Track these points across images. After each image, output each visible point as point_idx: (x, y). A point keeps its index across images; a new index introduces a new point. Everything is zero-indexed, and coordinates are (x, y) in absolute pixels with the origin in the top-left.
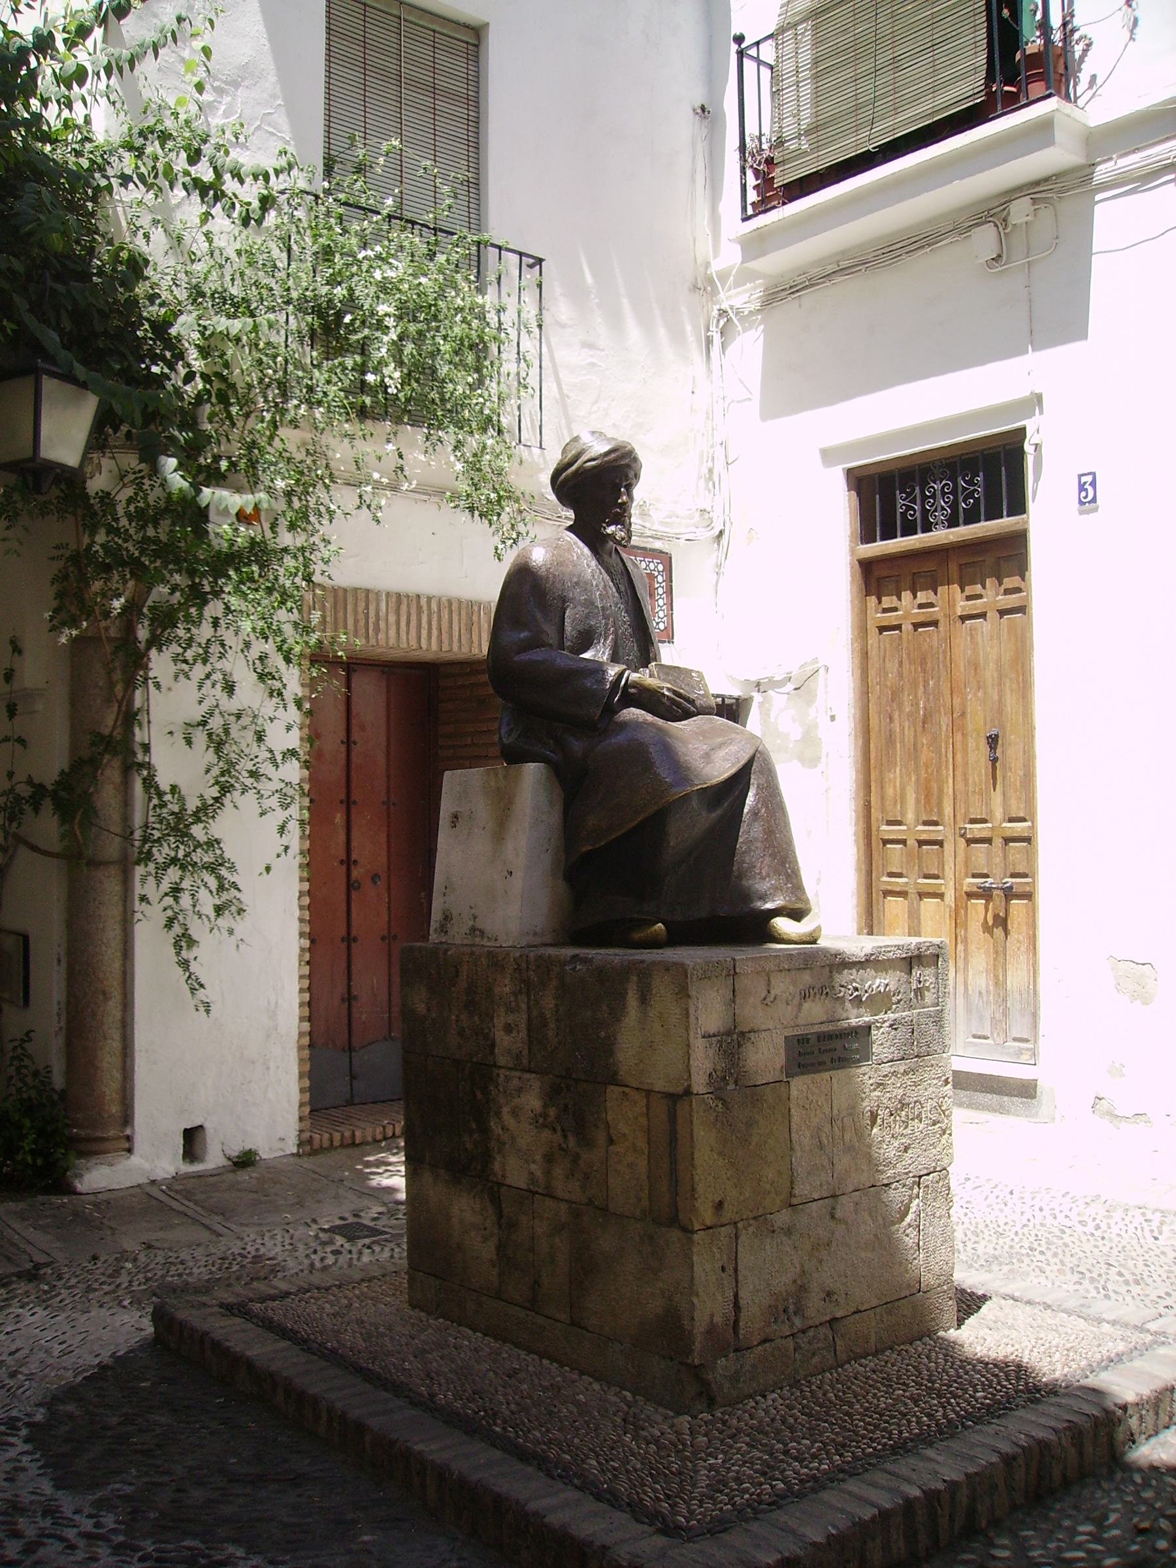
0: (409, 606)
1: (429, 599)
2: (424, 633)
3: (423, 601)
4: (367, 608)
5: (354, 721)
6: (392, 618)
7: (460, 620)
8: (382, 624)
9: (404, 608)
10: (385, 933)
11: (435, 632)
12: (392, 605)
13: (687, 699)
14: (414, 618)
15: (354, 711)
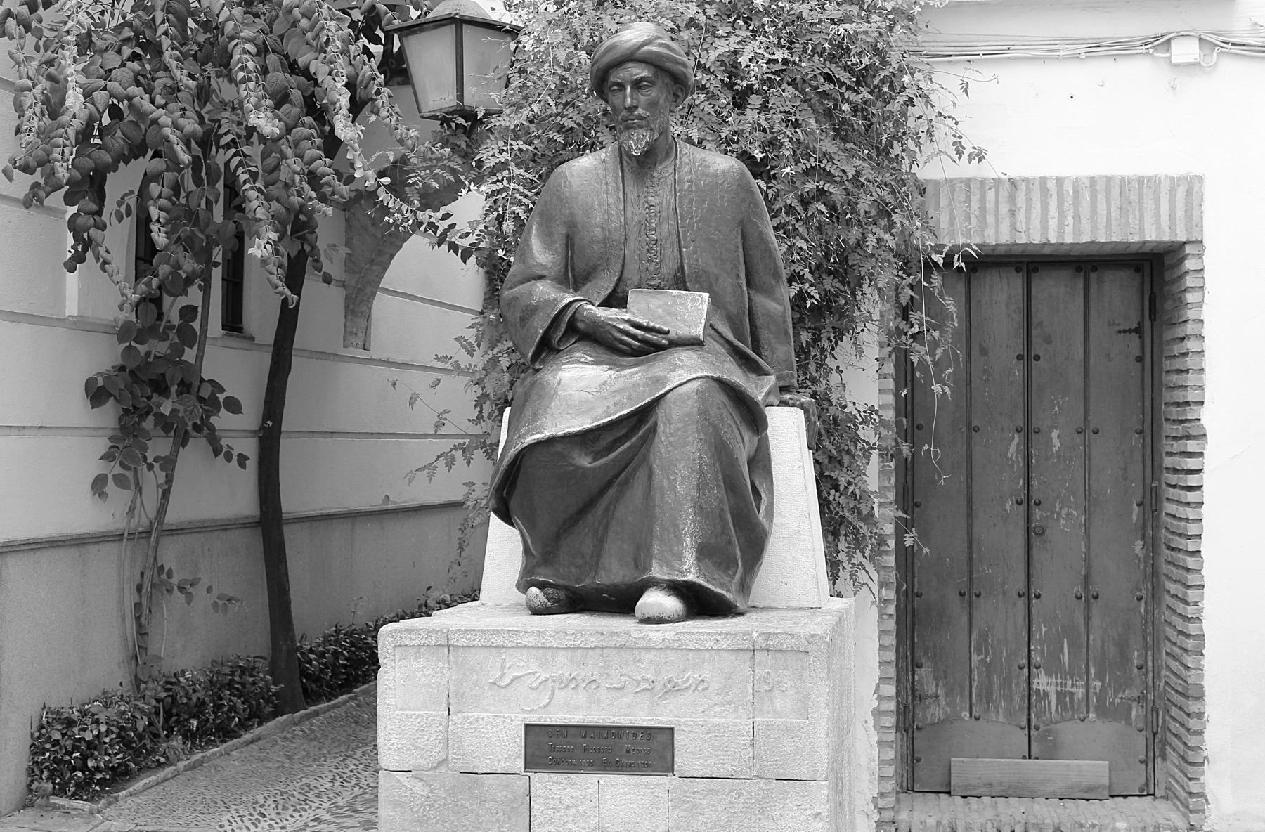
0: (1028, 191)
1: (1060, 181)
2: (1053, 224)
3: (1051, 185)
4: (968, 199)
5: (1034, 333)
6: (1004, 209)
7: (1109, 204)
8: (990, 219)
9: (1021, 198)
10: (1078, 589)
11: (1070, 220)
12: (1004, 193)
13: (659, 331)
14: (1037, 206)
15: (1035, 320)
